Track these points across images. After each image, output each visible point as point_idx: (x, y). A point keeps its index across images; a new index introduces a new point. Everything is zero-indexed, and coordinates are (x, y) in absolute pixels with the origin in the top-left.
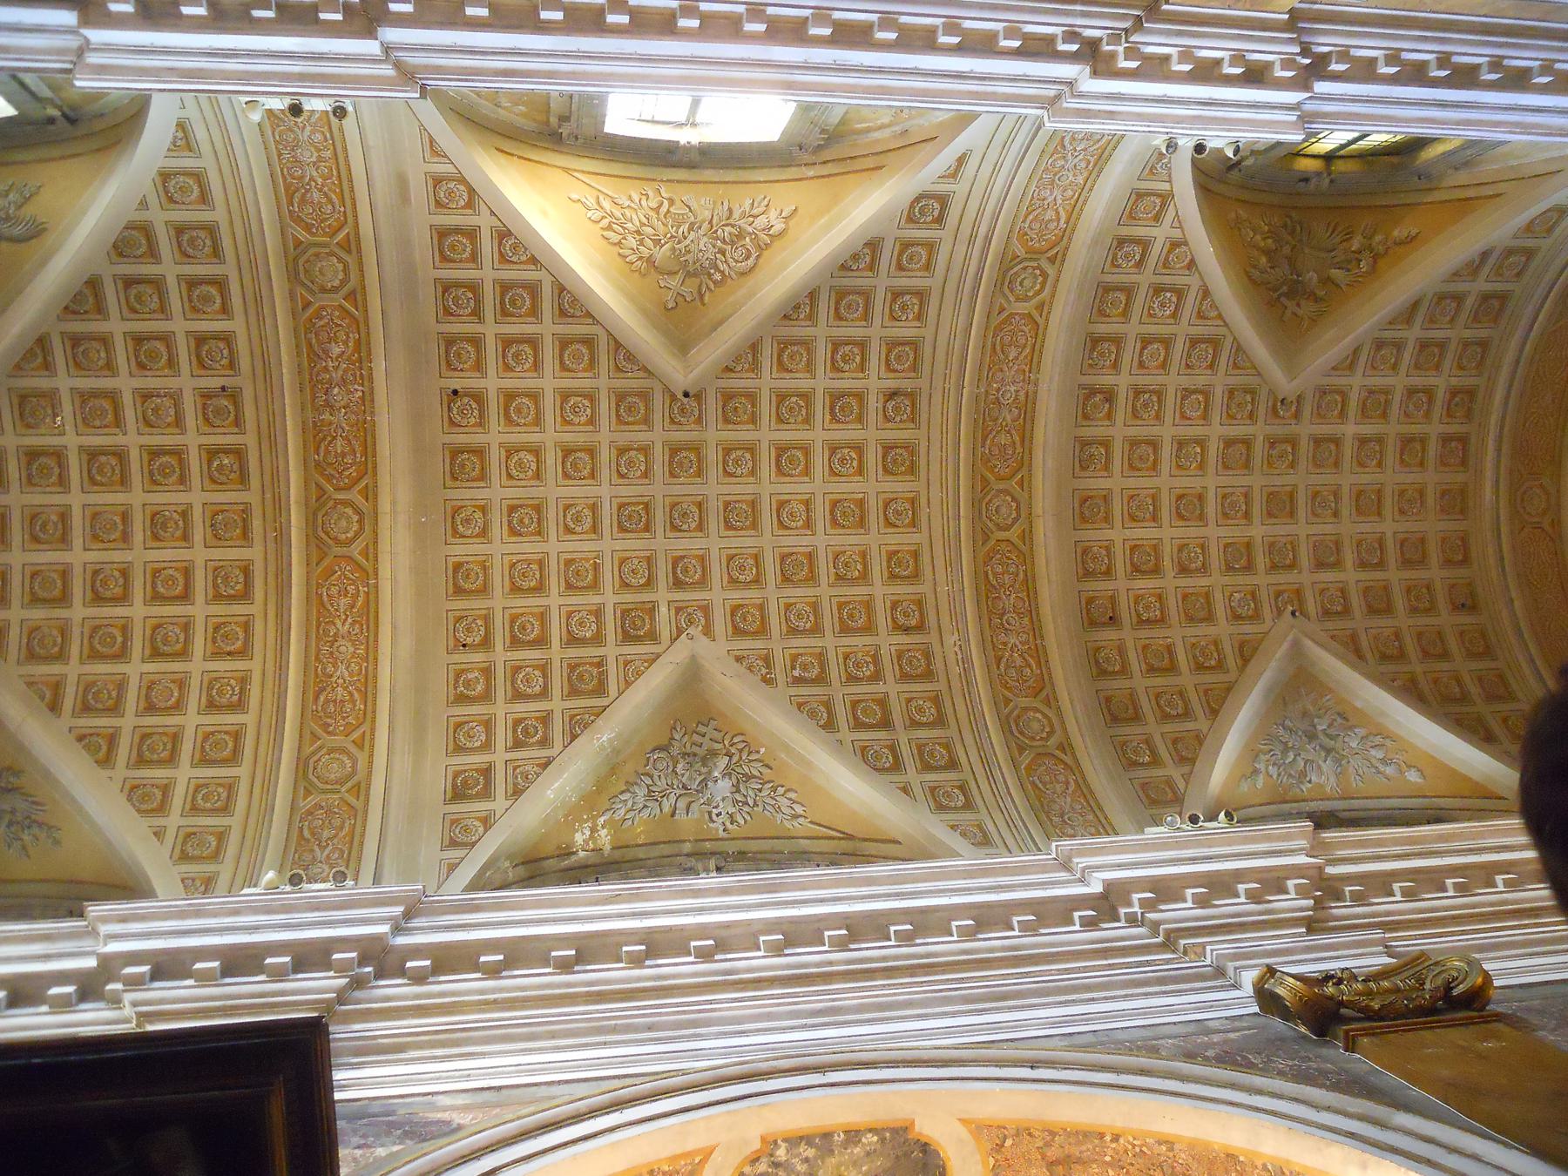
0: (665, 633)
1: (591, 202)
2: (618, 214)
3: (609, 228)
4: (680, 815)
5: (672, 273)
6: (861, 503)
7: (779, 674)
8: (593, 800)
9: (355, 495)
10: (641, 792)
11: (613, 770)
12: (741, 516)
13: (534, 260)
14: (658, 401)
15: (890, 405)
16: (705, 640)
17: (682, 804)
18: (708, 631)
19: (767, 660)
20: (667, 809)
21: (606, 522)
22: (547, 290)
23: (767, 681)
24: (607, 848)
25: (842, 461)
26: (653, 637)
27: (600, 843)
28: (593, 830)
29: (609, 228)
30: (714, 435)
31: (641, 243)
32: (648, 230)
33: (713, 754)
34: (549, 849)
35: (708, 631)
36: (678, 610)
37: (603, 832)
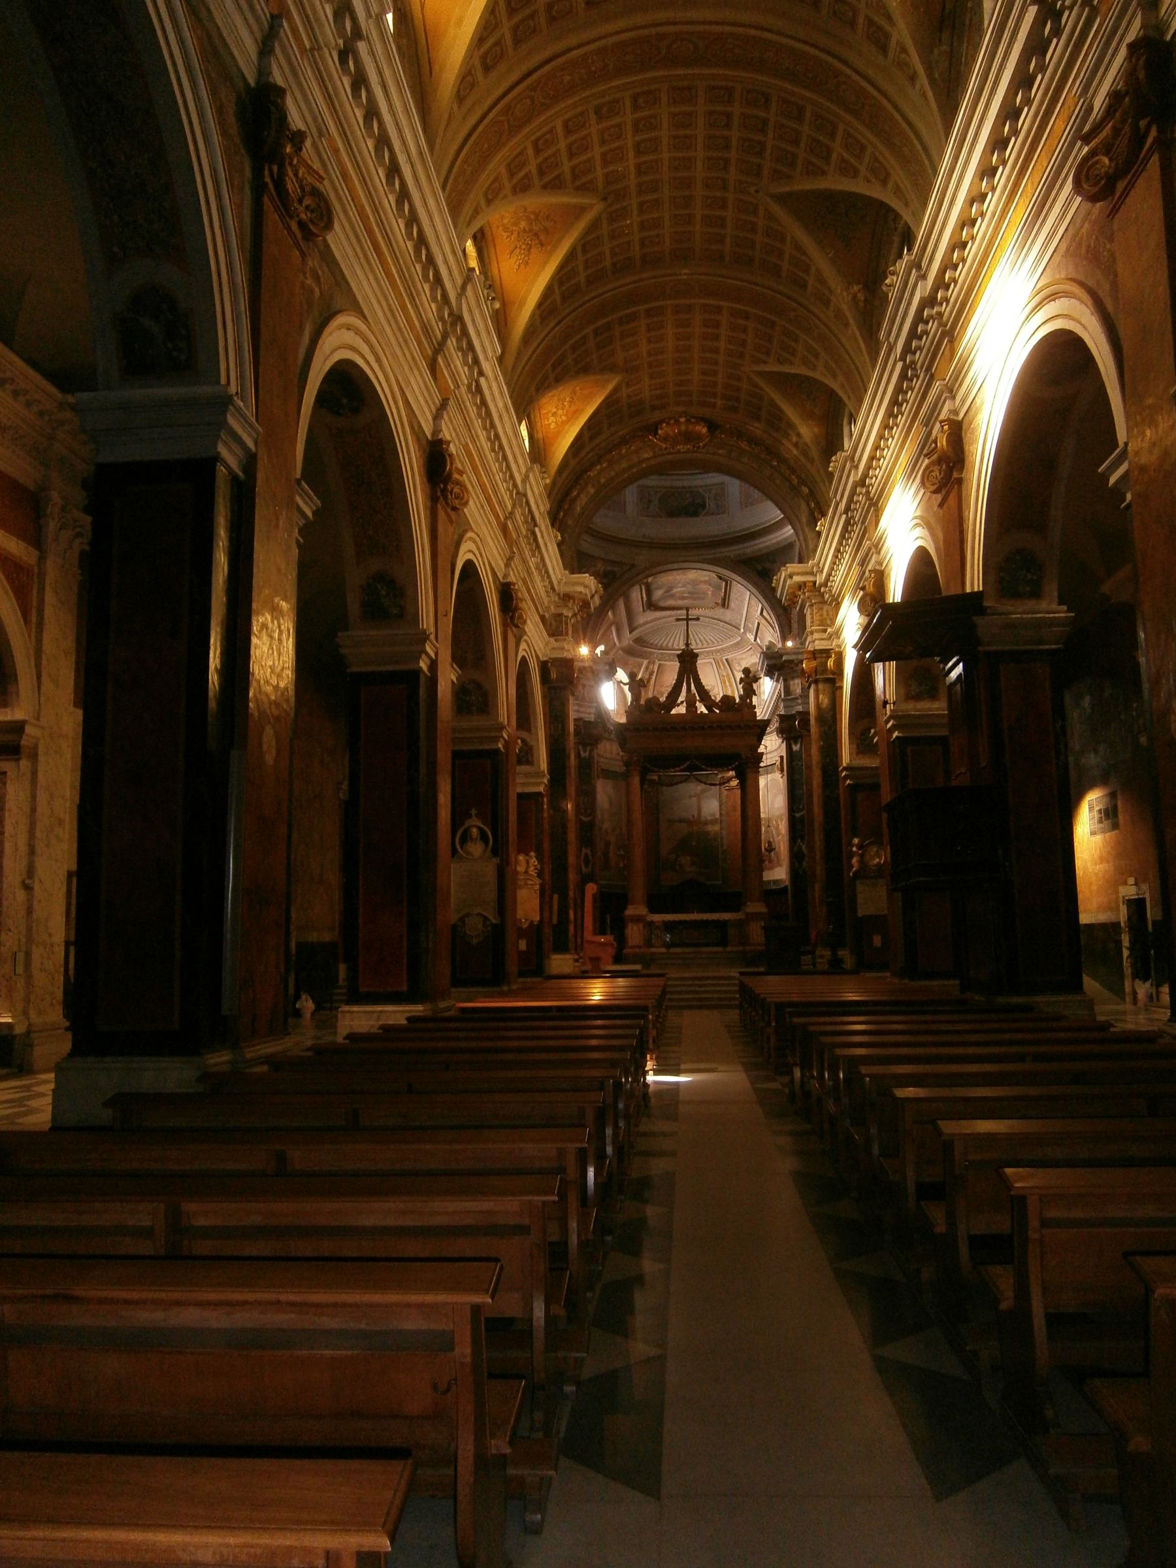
13: (493, 12)
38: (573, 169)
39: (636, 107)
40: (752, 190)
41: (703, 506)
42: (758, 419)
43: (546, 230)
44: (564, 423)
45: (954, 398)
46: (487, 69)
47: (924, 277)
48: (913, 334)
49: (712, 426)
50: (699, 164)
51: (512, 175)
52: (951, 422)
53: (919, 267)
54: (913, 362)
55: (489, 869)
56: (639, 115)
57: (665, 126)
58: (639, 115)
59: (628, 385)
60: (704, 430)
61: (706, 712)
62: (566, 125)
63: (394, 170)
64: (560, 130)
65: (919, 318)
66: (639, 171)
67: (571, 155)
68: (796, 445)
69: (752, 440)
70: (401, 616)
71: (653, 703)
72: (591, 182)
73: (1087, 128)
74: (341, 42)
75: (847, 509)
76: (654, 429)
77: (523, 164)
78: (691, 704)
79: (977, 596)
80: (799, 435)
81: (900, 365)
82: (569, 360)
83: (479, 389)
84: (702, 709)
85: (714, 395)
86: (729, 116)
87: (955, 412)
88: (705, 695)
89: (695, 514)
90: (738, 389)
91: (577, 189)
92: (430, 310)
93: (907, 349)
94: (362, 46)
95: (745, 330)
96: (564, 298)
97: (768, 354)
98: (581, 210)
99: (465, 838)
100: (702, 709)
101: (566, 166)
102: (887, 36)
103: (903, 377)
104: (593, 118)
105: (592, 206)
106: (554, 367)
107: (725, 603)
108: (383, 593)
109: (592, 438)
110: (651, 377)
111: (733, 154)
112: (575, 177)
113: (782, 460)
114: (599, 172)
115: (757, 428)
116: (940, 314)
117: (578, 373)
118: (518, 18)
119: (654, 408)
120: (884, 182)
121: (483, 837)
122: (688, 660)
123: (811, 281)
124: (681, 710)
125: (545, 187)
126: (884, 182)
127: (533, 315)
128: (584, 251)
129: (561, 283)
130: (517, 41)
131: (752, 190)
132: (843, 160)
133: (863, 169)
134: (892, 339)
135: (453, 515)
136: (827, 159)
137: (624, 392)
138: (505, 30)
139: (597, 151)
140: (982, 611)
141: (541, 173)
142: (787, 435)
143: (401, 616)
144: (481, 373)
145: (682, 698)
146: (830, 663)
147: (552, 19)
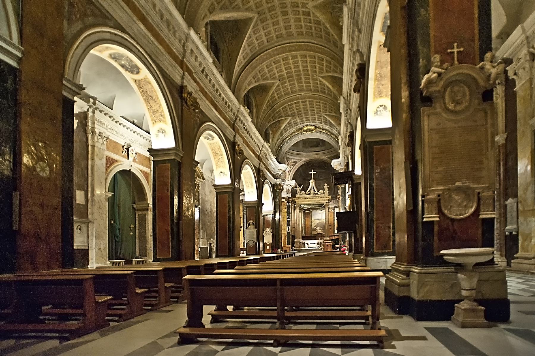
16: (309, 4)
18: (307, 4)
38: (270, 75)
49: (316, 127)
55: (255, 231)
56: (284, 62)
66: (287, 73)
67: (269, 72)
72: (275, 77)
85: (315, 120)
86: (306, 61)
91: (272, 79)
95: (320, 105)
99: (249, 225)
104: (273, 64)
111: (309, 68)
114: (277, 75)
119: (301, 124)
121: (253, 224)
131: (315, 76)
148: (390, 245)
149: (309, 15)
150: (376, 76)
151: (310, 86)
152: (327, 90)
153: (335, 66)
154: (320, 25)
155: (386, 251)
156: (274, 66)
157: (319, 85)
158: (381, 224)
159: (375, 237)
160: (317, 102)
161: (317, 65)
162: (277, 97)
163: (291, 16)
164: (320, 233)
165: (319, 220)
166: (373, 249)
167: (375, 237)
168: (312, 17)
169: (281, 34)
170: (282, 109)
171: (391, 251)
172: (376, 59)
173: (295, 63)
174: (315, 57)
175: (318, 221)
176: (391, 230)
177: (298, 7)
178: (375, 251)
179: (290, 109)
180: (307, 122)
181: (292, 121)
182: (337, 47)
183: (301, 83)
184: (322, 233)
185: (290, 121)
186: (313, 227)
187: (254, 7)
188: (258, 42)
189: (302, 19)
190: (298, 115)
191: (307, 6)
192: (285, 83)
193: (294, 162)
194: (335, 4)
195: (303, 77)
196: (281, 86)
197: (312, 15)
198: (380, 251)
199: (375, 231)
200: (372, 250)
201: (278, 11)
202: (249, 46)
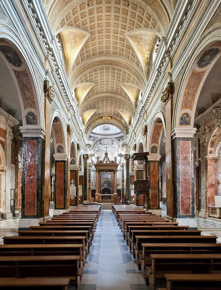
0: (123, 37)
1: (69, 51)
2: (70, 47)
3: (72, 48)
4: (148, 42)
5: (76, 39)
6: (107, 7)
7: (132, 27)
8: (143, 54)
9: (105, 62)
10: (143, 46)
11: (140, 50)
12: (108, 25)
13: (78, 56)
14: (92, 37)
15: (90, 5)
16: (125, 33)
17: (146, 42)
19: (130, 27)
20: (147, 44)
21: (108, 40)
22: (80, 53)
23: (132, 29)
24: (149, 52)
25: (100, 11)
26: (124, 39)
27: (148, 53)
28: (146, 54)
29: (72, 48)
30: (97, 29)
31: (73, 44)
32: (71, 43)
33: (141, 37)
34: (146, 61)
35: (124, 33)
36: (121, 34)
37: (147, 52)
38: (90, 79)
39: (100, 70)
40: (118, 83)
41: (110, 129)
42: (119, 117)
43: (85, 88)
44: (87, 116)
45: (146, 122)
46: (77, 65)
47: (143, 103)
48: (141, 111)
50: (110, 79)
51: (80, 80)
52: (146, 126)
53: (142, 102)
54: (141, 115)
56: (101, 71)
57: (105, 73)
58: (101, 71)
59: (98, 111)
60: (110, 118)
61: (109, 163)
62: (89, 72)
63: (63, 86)
64: (88, 73)
65: (142, 109)
68: (124, 121)
69: (118, 120)
70: (63, 152)
71: (101, 162)
73: (162, 92)
74: (56, 70)
75: (131, 134)
76: (102, 117)
77: (82, 78)
78: (107, 162)
79: (148, 152)
80: (125, 120)
81: (139, 115)
82: (89, 107)
83: (75, 116)
84: (108, 162)
87: (146, 124)
88: (109, 160)
89: (108, 130)
90: (115, 112)
92: (68, 105)
93: (140, 113)
94: (59, 70)
95: (117, 104)
96: (88, 98)
97: (120, 107)
98: (91, 85)
100: (108, 162)
101: (89, 79)
102: (139, 64)
103: (140, 116)
104: (93, 72)
105: (93, 84)
106: (86, 108)
107: (112, 144)
108: (60, 148)
109: (92, 119)
110: (102, 110)
111: (115, 78)
112: (90, 80)
113: (122, 124)
114: (94, 79)
115: (118, 118)
116: (145, 109)
117: (90, 109)
118: (82, 57)
119: (102, 114)
120: (138, 85)
122: (106, 154)
123: (127, 97)
124: (105, 162)
125: (85, 82)
126: (138, 85)
127: (83, 101)
128: (91, 91)
129: (88, 96)
130: (82, 61)
131: (118, 83)
132: (132, 81)
133: (135, 83)
134: (138, 111)
135: (70, 135)
136: (130, 80)
137: (97, 112)
138: (80, 59)
139: (94, 76)
140: (148, 155)
141: (85, 80)
142: (123, 120)
143: (63, 152)
144: (75, 113)
145: (105, 160)
146: (128, 156)
147: (87, 57)
148: (190, 211)
149: (124, 41)
150: (186, 93)
151: (113, 90)
152: (124, 94)
153: (133, 79)
154: (130, 49)
155: (188, 215)
156: (94, 73)
157: (119, 90)
158: (184, 195)
159: (181, 204)
160: (115, 101)
161: (121, 76)
162: (91, 95)
163: (111, 39)
164: (106, 188)
165: (106, 179)
166: (180, 213)
167: (181, 204)
168: (125, 43)
169: (103, 51)
170: (93, 103)
171: (191, 214)
172: (188, 82)
173: (107, 73)
174: (115, 69)
175: (105, 180)
176: (191, 200)
177: (117, 33)
178: (181, 214)
179: (97, 103)
180: (106, 114)
181: (97, 112)
182: (138, 67)
183: (108, 87)
184: (108, 188)
185: (96, 112)
186: (102, 183)
187: (89, 28)
188: (87, 54)
189: (118, 43)
190: (102, 108)
191: (124, 34)
192: (98, 85)
193: (94, 139)
194: (143, 36)
195: (110, 83)
196: (95, 88)
197: (126, 40)
198: (184, 215)
199: (181, 200)
200: (179, 214)
201: (104, 34)
202: (81, 56)
